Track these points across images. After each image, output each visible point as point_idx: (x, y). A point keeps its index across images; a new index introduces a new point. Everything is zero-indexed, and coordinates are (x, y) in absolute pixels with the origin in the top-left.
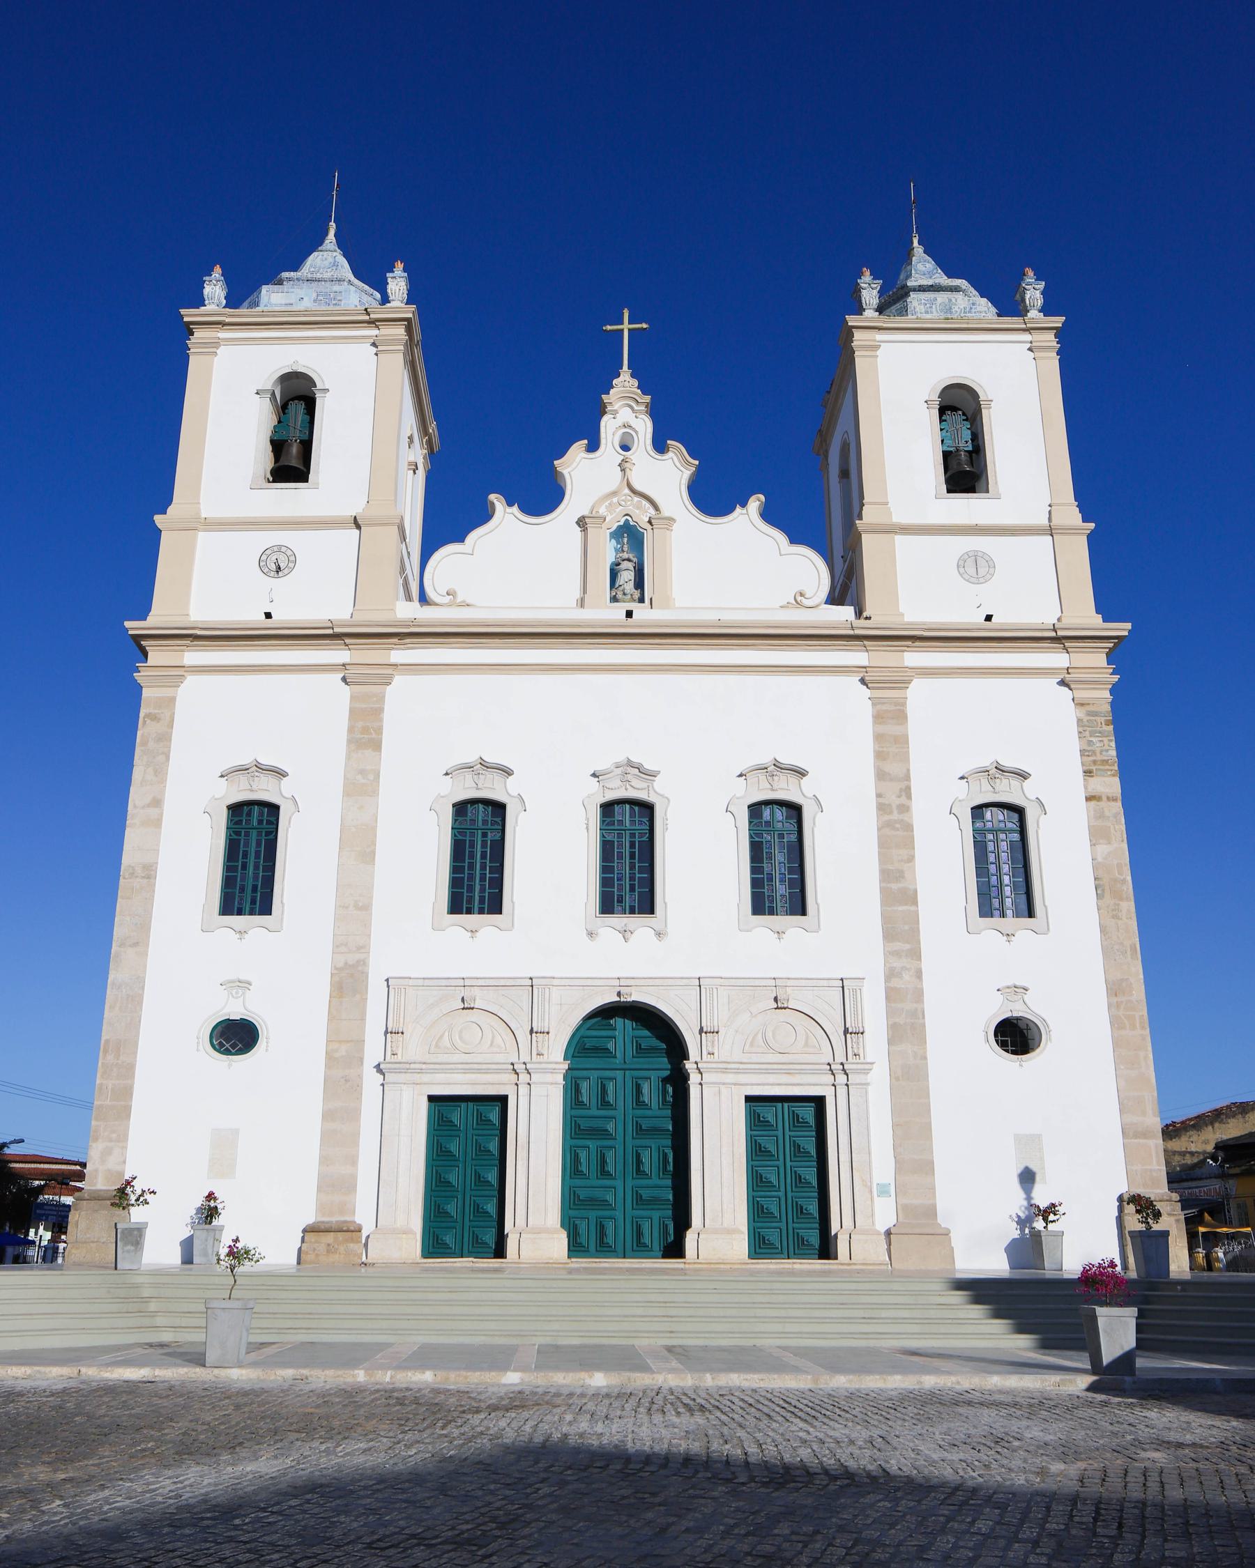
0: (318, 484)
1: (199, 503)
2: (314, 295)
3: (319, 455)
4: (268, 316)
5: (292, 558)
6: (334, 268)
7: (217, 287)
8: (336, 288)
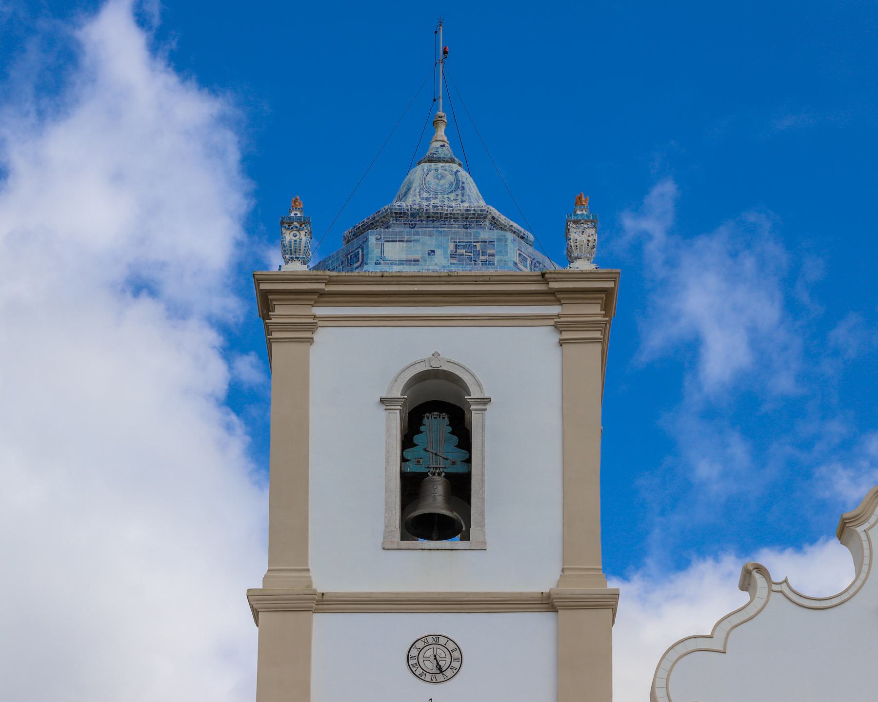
0: (484, 543)
1: (308, 570)
2: (451, 247)
3: (483, 499)
4: (388, 283)
5: (456, 654)
6: (459, 192)
7: (303, 233)
8: (485, 234)
